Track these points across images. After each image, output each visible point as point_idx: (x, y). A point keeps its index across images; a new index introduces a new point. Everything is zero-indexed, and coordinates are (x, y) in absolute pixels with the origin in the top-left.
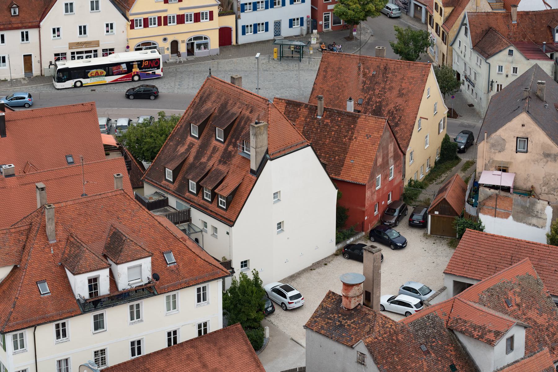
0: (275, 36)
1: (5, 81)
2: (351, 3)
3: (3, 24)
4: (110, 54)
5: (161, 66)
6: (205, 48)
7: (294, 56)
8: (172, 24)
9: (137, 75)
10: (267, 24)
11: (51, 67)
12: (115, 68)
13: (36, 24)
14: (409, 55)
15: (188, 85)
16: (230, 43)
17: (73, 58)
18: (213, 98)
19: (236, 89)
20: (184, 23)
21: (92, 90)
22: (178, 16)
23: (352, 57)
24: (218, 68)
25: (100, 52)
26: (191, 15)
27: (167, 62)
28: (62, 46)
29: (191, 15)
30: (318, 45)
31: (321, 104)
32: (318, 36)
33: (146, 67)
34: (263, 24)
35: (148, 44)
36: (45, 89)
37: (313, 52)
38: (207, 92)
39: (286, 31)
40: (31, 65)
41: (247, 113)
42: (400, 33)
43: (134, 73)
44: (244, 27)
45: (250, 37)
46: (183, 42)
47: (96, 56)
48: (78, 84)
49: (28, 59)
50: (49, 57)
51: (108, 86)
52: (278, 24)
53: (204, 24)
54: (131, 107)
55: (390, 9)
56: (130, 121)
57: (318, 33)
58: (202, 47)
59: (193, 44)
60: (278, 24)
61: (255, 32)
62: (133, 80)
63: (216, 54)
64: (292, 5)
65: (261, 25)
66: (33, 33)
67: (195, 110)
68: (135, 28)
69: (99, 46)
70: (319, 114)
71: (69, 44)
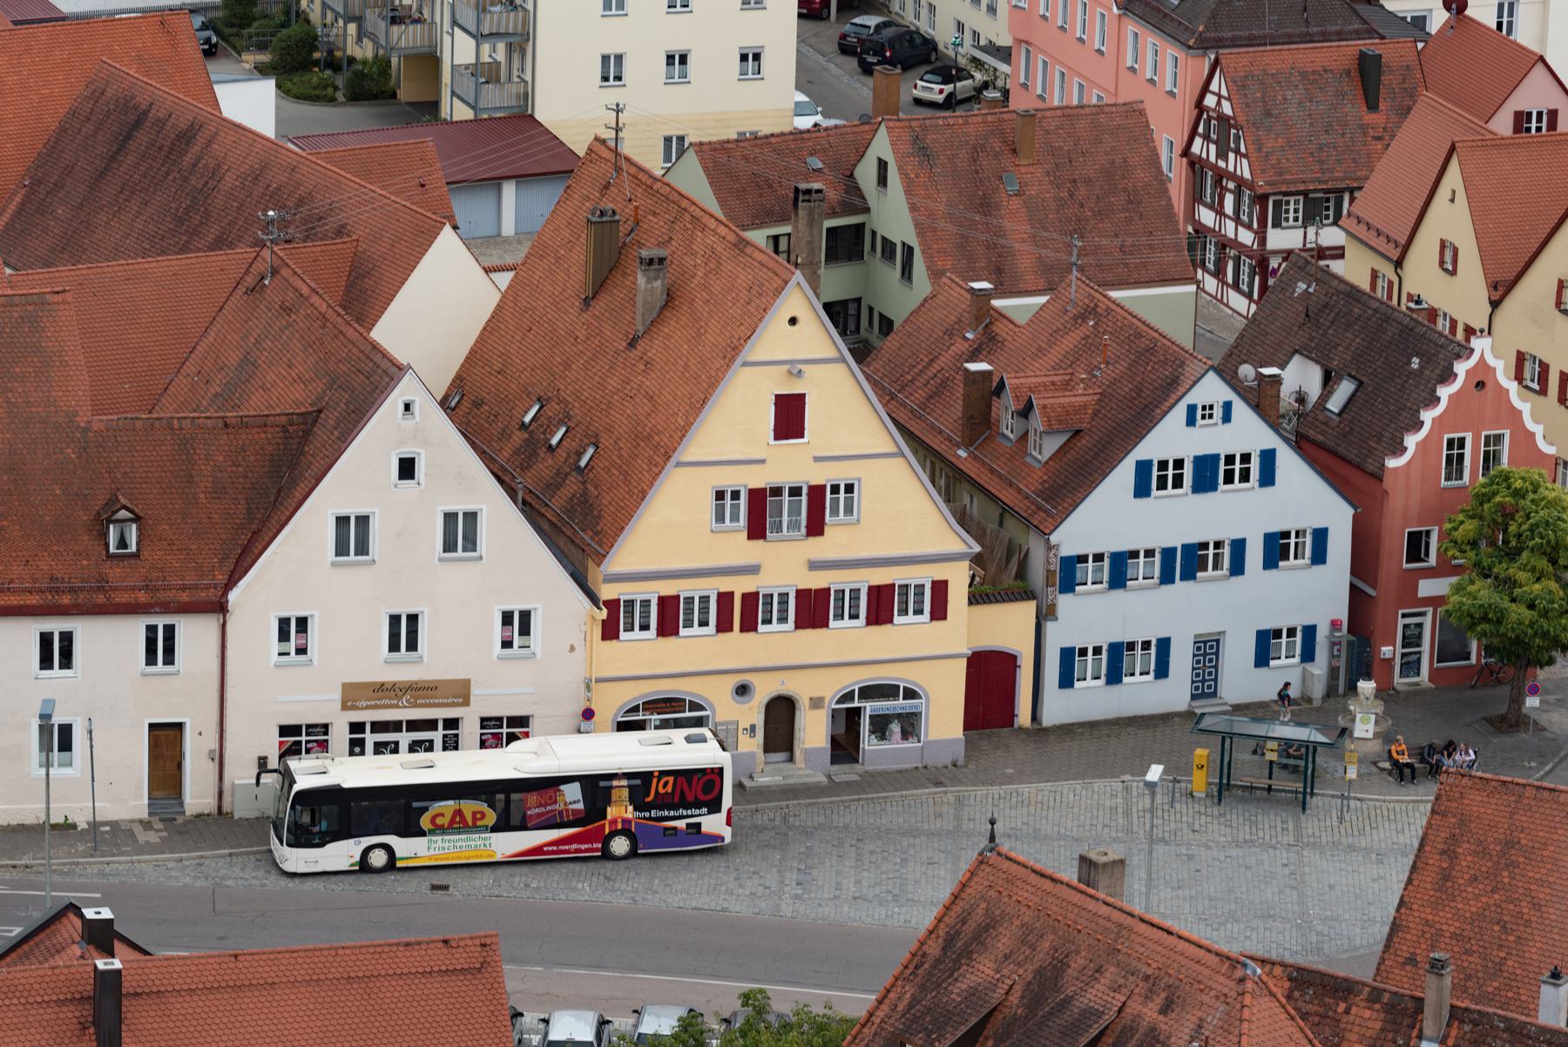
0: (1193, 697)
1: (67, 827)
2: (1522, 576)
3: (72, 590)
4: (512, 738)
5: (727, 801)
6: (905, 735)
7: (1276, 784)
8: (775, 626)
9: (626, 832)
10: (1164, 645)
11: (267, 779)
12: (532, 798)
13: (212, 595)
15: (838, 887)
17: (356, 747)
18: (1004, 940)
19: (1105, 910)
20: (825, 624)
21: (434, 887)
22: (802, 595)
24: (958, 818)
25: (470, 730)
26: (855, 593)
27: (747, 783)
28: (312, 695)
29: (855, 593)
31: (1440, 989)
33: (663, 802)
34: (1146, 645)
36: (237, 871)
37: (1359, 775)
38: (978, 916)
39: (1242, 680)
40: (180, 766)
41: (1149, 1012)
43: (614, 822)
44: (1067, 655)
45: (1091, 699)
46: (816, 703)
47: (451, 744)
48: (378, 859)
49: (166, 740)
50: (254, 738)
51: (500, 871)
52: (1208, 649)
53: (911, 631)
54: (599, 967)
56: (603, 1023)
57: (1380, 693)
58: (895, 728)
59: (855, 714)
60: (1208, 649)
61: (1114, 677)
62: (607, 855)
63: (948, 762)
64: (1274, 572)
65: (1139, 651)
66: (195, 634)
67: (923, 988)
68: (623, 635)
69: (466, 703)
70: (1427, 1031)
71: (345, 686)
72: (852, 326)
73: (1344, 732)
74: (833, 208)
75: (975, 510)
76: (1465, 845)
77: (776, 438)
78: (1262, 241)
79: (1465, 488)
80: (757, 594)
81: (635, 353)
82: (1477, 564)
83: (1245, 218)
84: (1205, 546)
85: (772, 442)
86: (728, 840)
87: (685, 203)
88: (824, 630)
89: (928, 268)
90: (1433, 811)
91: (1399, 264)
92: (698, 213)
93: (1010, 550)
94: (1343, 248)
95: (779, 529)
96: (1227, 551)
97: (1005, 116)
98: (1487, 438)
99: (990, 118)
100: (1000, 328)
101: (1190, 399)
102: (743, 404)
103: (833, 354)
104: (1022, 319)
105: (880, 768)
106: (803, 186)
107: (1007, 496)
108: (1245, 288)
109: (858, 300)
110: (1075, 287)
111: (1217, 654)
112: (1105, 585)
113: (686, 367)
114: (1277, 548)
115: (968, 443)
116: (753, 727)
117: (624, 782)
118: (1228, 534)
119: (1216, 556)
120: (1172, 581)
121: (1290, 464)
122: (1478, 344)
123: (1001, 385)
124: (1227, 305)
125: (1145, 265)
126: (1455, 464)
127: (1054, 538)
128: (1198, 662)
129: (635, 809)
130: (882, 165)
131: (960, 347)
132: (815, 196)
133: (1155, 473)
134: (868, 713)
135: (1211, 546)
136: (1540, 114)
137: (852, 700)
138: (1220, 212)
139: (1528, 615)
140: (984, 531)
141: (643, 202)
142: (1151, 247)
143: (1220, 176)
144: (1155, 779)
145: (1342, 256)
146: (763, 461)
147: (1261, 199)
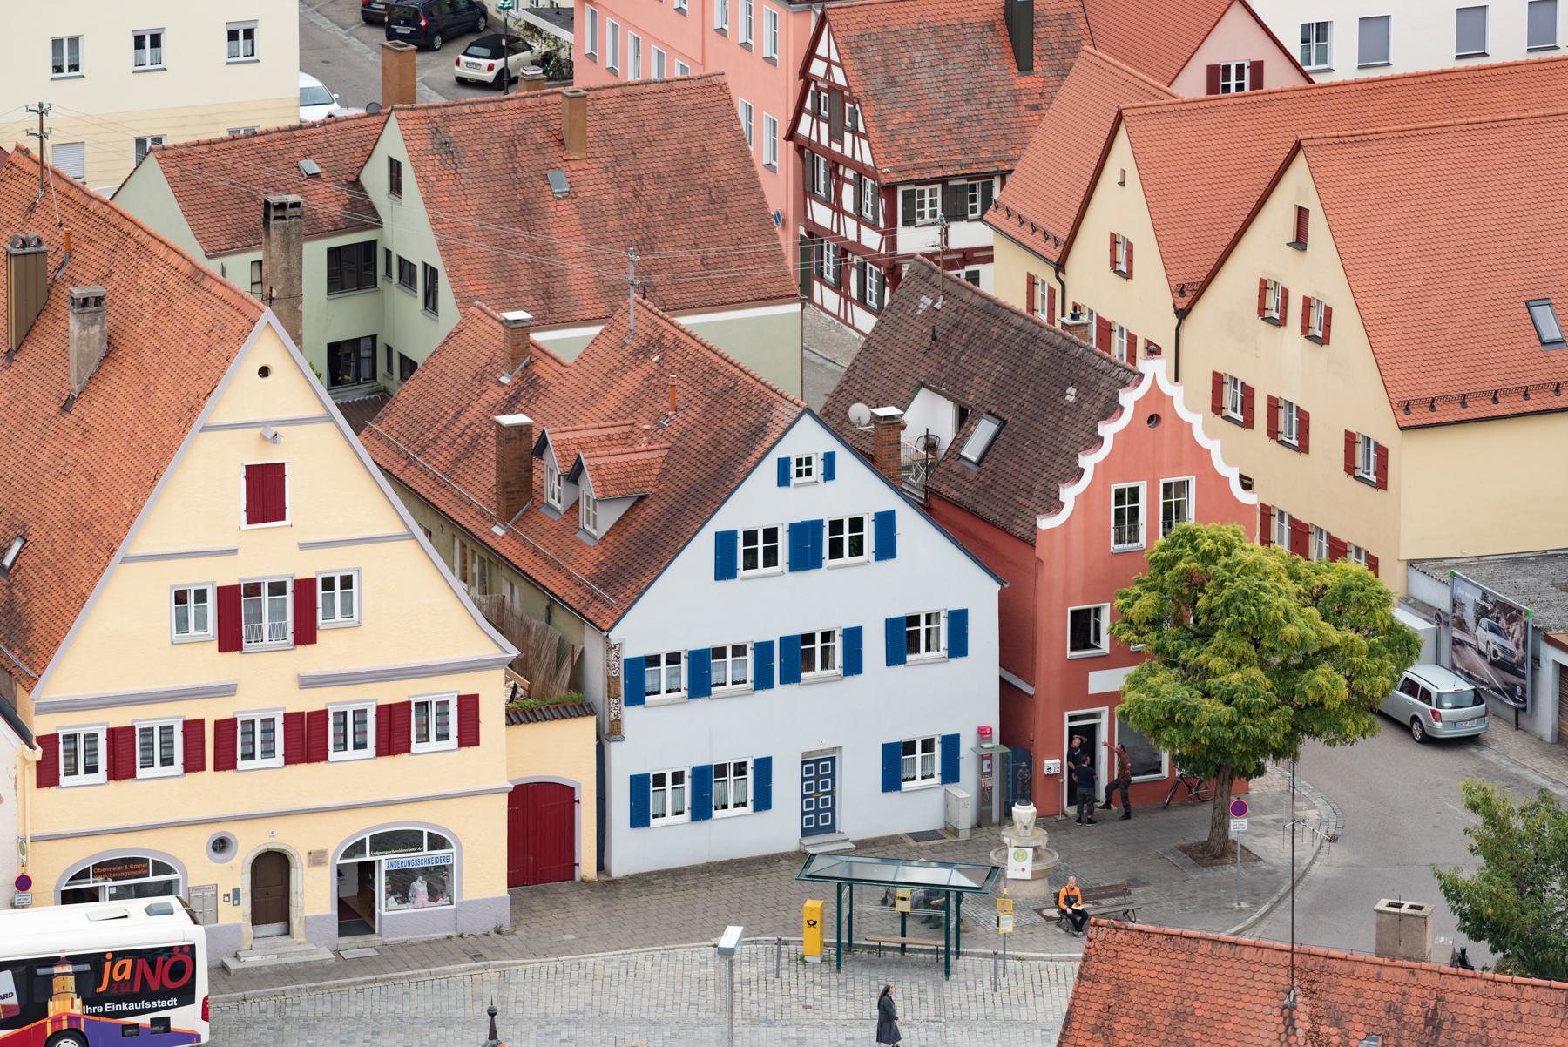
0: (805, 833)
2: (1217, 663)
5: (202, 988)
6: (434, 895)
7: (911, 941)
8: (259, 761)
10: (764, 767)
14: (1543, 944)
16: (565, 867)
20: (325, 758)
22: (290, 719)
23: (1248, 954)
26: (360, 715)
27: (232, 964)
29: (360, 715)
30: (1040, 889)
32: (1041, 837)
33: (120, 993)
34: (740, 769)
35: (132, 865)
39: (864, 808)
42: (1492, 819)
44: (639, 786)
45: (675, 839)
46: (317, 858)
52: (820, 771)
53: (432, 763)
55: (1426, 696)
57: (1042, 820)
58: (420, 886)
59: (367, 869)
61: (701, 811)
63: (490, 928)
64: (899, 669)
65: (731, 775)
72: (365, 371)
73: (995, 871)
74: (335, 223)
75: (517, 605)
76: (1124, 1019)
77: (249, 522)
78: (892, 243)
79: (1141, 551)
80: (235, 720)
81: (69, 420)
82: (1160, 650)
83: (869, 215)
84: (809, 638)
85: (245, 526)
86: (205, 1039)
87: (127, 227)
88: (323, 764)
89: (457, 295)
90: (1081, 976)
91: (1060, 266)
92: (144, 238)
93: (562, 651)
94: (991, 248)
95: (259, 638)
96: (838, 644)
97: (549, 99)
98: (1167, 487)
99: (529, 102)
100: (542, 369)
101: (780, 451)
102: (205, 480)
103: (317, 411)
104: (569, 357)
105: (402, 939)
106: (274, 199)
107: (555, 583)
108: (873, 304)
109: (374, 338)
110: (635, 314)
111: (833, 776)
112: (684, 693)
113: (133, 435)
114: (904, 638)
115: (506, 516)
116: (236, 893)
117: (69, 969)
118: (838, 622)
119: (825, 650)
120: (770, 685)
121: (912, 528)
122: (1154, 370)
123: (543, 442)
124: (852, 327)
125: (734, 281)
126: (1127, 519)
127: (614, 636)
128: (809, 787)
129: (84, 1004)
130: (395, 167)
131: (494, 395)
132: (290, 211)
133: (741, 548)
134: (384, 868)
135: (818, 638)
136: (1240, 68)
137: (363, 852)
138: (838, 209)
139: (1225, 712)
140: (528, 629)
141: (78, 226)
142: (741, 257)
143: (835, 163)
144: (732, 945)
145: (990, 259)
146: (234, 552)
147: (888, 190)
